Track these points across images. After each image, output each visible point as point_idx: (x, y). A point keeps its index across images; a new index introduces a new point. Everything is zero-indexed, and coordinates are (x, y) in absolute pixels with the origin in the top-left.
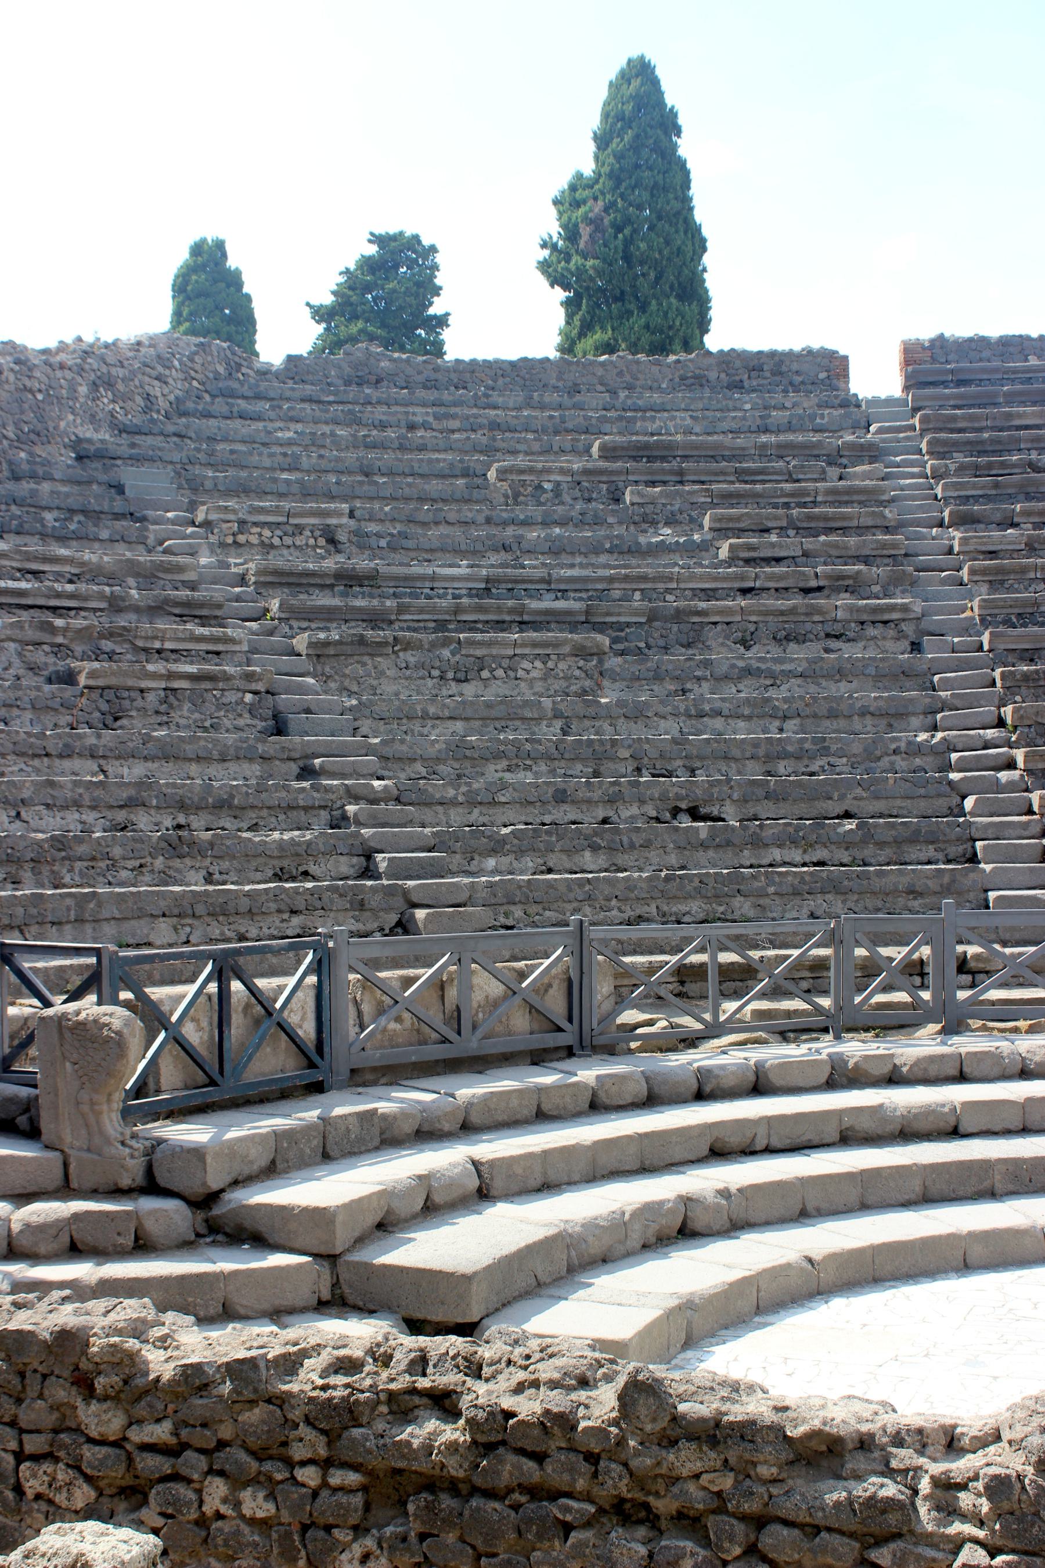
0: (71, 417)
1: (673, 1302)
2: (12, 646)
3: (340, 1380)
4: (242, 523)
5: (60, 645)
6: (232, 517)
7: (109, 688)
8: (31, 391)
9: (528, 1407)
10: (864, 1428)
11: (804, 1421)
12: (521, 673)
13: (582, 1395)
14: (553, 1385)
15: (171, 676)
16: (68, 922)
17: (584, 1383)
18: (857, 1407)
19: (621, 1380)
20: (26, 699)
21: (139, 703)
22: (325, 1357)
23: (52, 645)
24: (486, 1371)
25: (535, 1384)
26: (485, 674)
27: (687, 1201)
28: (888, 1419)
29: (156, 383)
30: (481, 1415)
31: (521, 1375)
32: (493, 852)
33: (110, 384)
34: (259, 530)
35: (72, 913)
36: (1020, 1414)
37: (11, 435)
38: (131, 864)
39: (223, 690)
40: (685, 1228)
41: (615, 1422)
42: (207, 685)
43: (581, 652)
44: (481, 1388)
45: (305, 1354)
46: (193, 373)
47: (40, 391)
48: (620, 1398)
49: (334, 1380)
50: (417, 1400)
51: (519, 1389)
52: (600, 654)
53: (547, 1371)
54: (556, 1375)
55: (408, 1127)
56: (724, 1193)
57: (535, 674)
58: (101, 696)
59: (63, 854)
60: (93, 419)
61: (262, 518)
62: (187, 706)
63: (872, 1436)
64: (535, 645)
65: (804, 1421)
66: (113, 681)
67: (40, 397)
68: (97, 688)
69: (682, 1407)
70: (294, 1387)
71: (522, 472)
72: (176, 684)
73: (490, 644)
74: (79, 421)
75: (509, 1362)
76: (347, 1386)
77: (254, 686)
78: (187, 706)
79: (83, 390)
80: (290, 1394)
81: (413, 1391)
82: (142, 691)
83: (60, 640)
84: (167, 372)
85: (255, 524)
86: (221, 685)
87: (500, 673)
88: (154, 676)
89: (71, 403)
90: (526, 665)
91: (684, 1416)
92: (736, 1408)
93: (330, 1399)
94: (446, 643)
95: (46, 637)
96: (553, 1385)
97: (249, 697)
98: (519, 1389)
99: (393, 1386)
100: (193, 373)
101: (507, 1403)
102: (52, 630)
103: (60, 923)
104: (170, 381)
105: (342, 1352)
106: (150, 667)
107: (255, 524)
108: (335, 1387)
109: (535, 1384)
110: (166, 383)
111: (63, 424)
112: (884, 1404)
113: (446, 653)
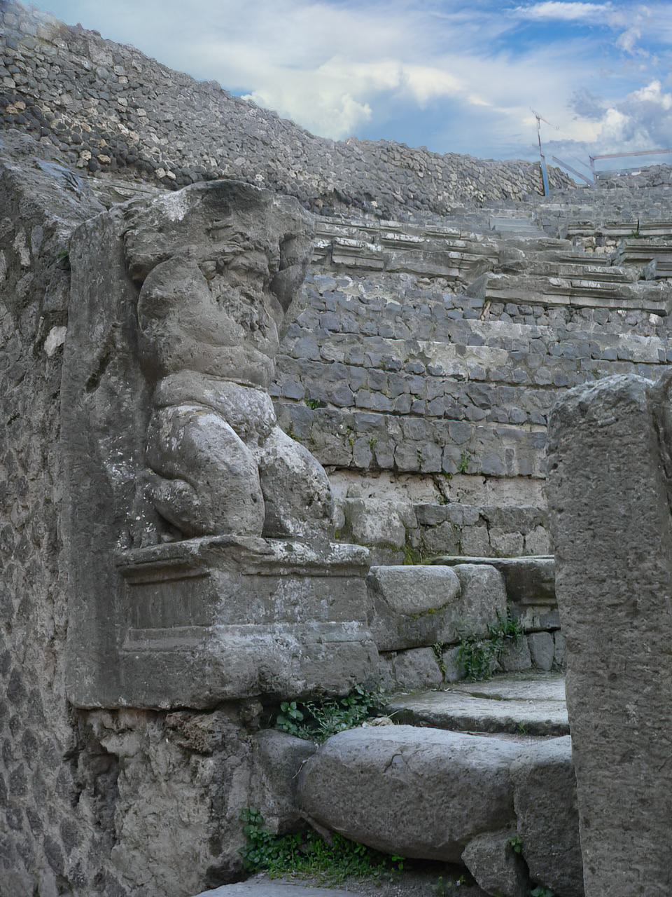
0: (446, 194)
4: (599, 235)
5: (456, 279)
6: (591, 232)
7: (511, 301)
8: (413, 169)
15: (574, 292)
16: (508, 477)
20: (425, 307)
23: (449, 278)
29: (508, 183)
33: (474, 177)
34: (614, 242)
35: (515, 463)
37: (399, 197)
39: (627, 309)
42: (612, 304)
46: (534, 182)
47: (421, 171)
58: (504, 310)
59: (488, 412)
60: (463, 198)
61: (616, 232)
67: (421, 175)
68: (500, 300)
74: (452, 198)
77: (658, 306)
79: (454, 177)
82: (546, 307)
83: (455, 273)
84: (515, 177)
85: (611, 237)
86: (624, 304)
88: (557, 290)
89: (445, 184)
95: (443, 270)
97: (654, 318)
100: (534, 182)
102: (449, 263)
103: (497, 478)
104: (519, 184)
107: (611, 237)
110: (516, 185)
111: (440, 198)
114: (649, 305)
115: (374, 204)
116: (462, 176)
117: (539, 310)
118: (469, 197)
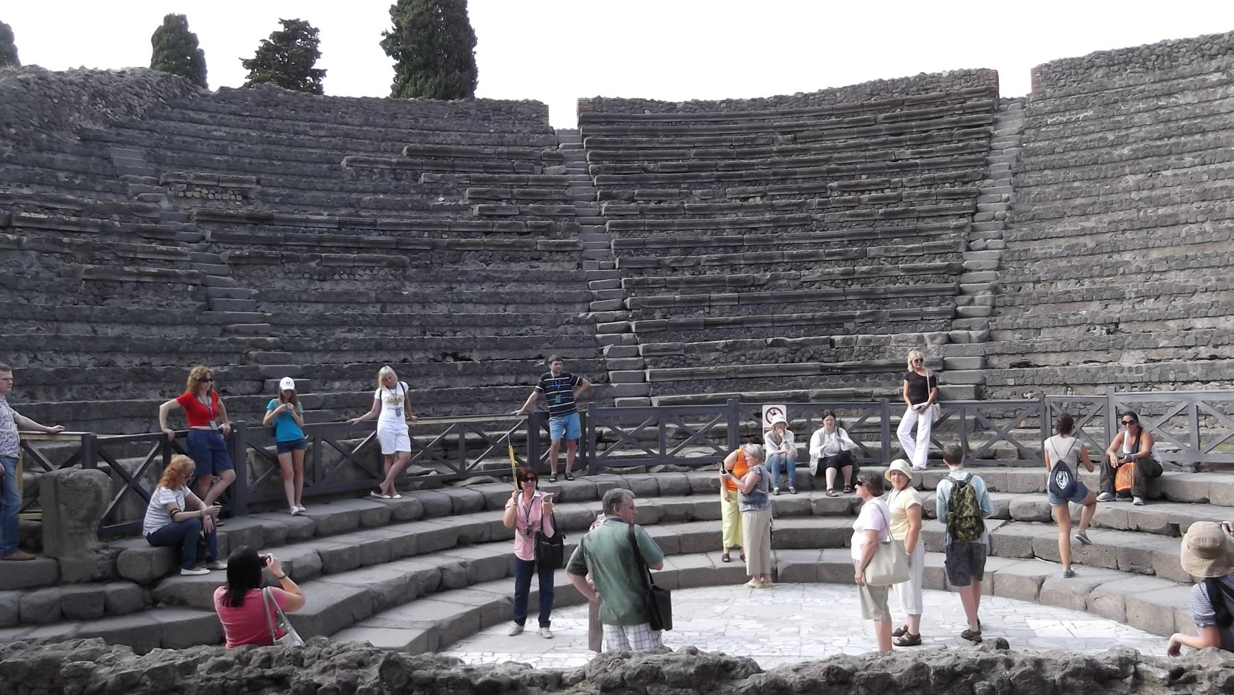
1: (430, 626)
2: (33, 253)
3: (218, 675)
4: (189, 184)
8: (49, 97)
9: (329, 681)
10: (514, 677)
11: (481, 676)
12: (357, 277)
13: (361, 671)
14: (343, 667)
17: (361, 664)
18: (511, 667)
19: (381, 661)
21: (119, 290)
22: (210, 662)
23: (62, 253)
24: (306, 662)
25: (334, 667)
26: (337, 277)
27: (442, 570)
28: (526, 672)
30: (302, 688)
31: (326, 663)
32: (339, 378)
33: (103, 96)
36: (595, 664)
37: (36, 123)
38: (111, 386)
40: (438, 585)
41: (377, 685)
42: (165, 280)
43: (391, 264)
44: (302, 672)
45: (197, 661)
48: (380, 671)
49: (214, 675)
50: (265, 682)
51: (324, 671)
52: (404, 266)
53: (340, 659)
54: (344, 661)
55: (281, 535)
56: (463, 565)
57: (365, 277)
60: (92, 117)
62: (151, 292)
63: (517, 681)
64: (365, 260)
65: (481, 676)
66: (102, 276)
69: (416, 673)
70: (192, 681)
71: (361, 162)
72: (144, 280)
73: (340, 260)
75: (319, 657)
76: (223, 678)
77: (194, 281)
78: (151, 292)
79: (85, 98)
80: (189, 685)
81: (262, 677)
82: (121, 282)
83: (67, 251)
85: (198, 186)
87: (345, 276)
88: (130, 274)
90: (360, 272)
91: (417, 677)
92: (446, 671)
93: (212, 686)
94: (313, 258)
96: (343, 667)
97: (190, 288)
98: (324, 671)
99: (251, 676)
101: (316, 680)
102: (62, 244)
105: (222, 658)
106: (127, 269)
107: (198, 186)
108: (216, 679)
109: (334, 667)
111: (71, 119)
112: (526, 665)
113: (313, 264)
114: (188, 281)
115: (13, 131)
116: (93, 97)
117: (117, 284)
118: (97, 115)
